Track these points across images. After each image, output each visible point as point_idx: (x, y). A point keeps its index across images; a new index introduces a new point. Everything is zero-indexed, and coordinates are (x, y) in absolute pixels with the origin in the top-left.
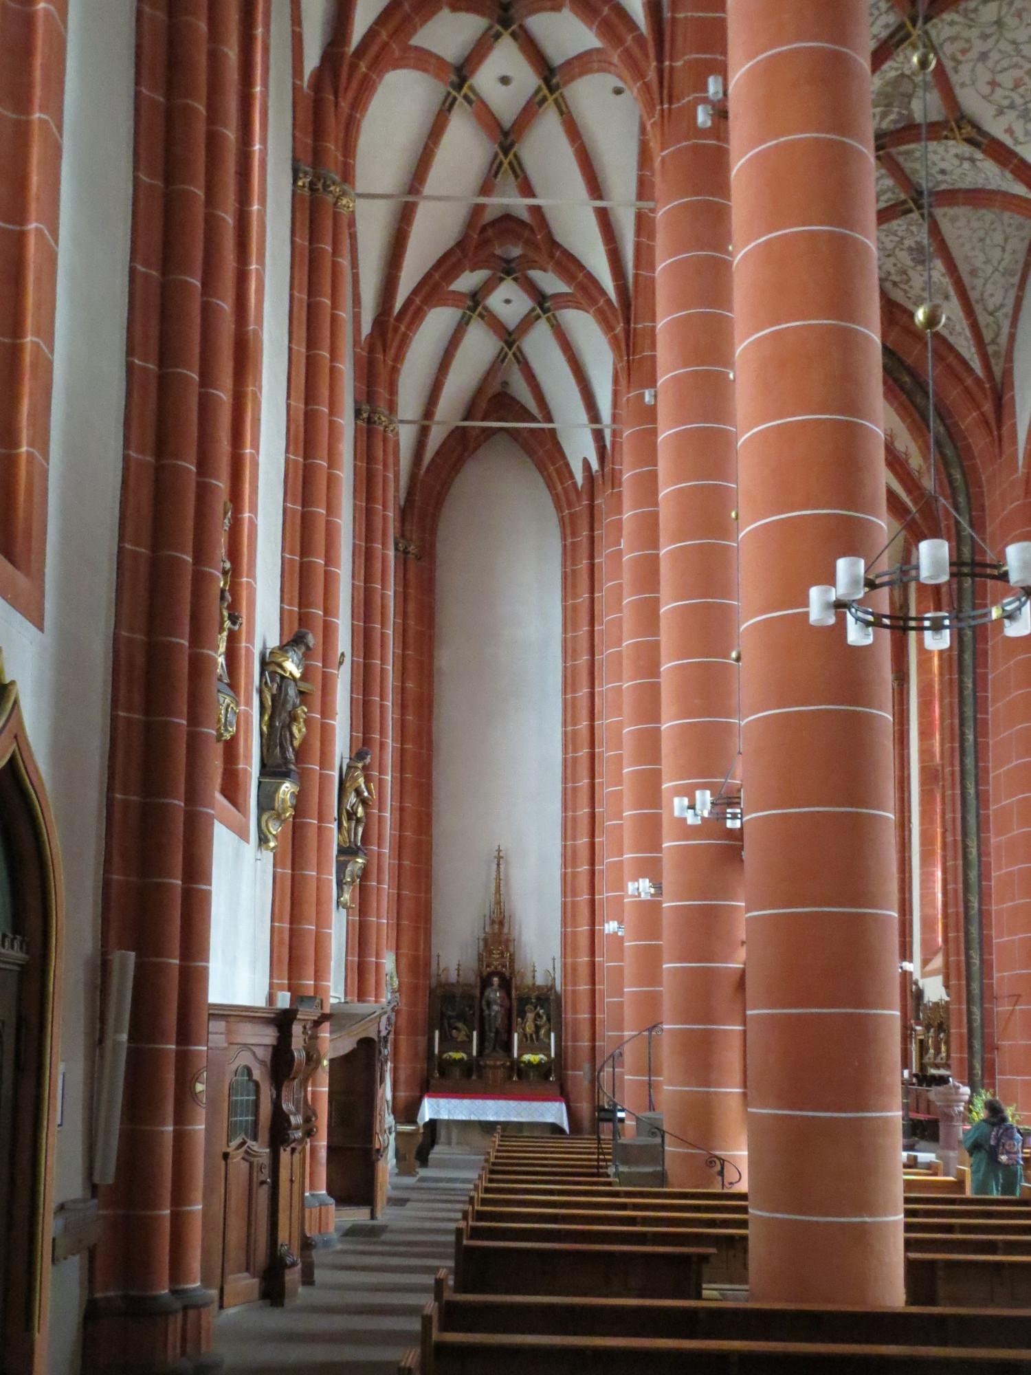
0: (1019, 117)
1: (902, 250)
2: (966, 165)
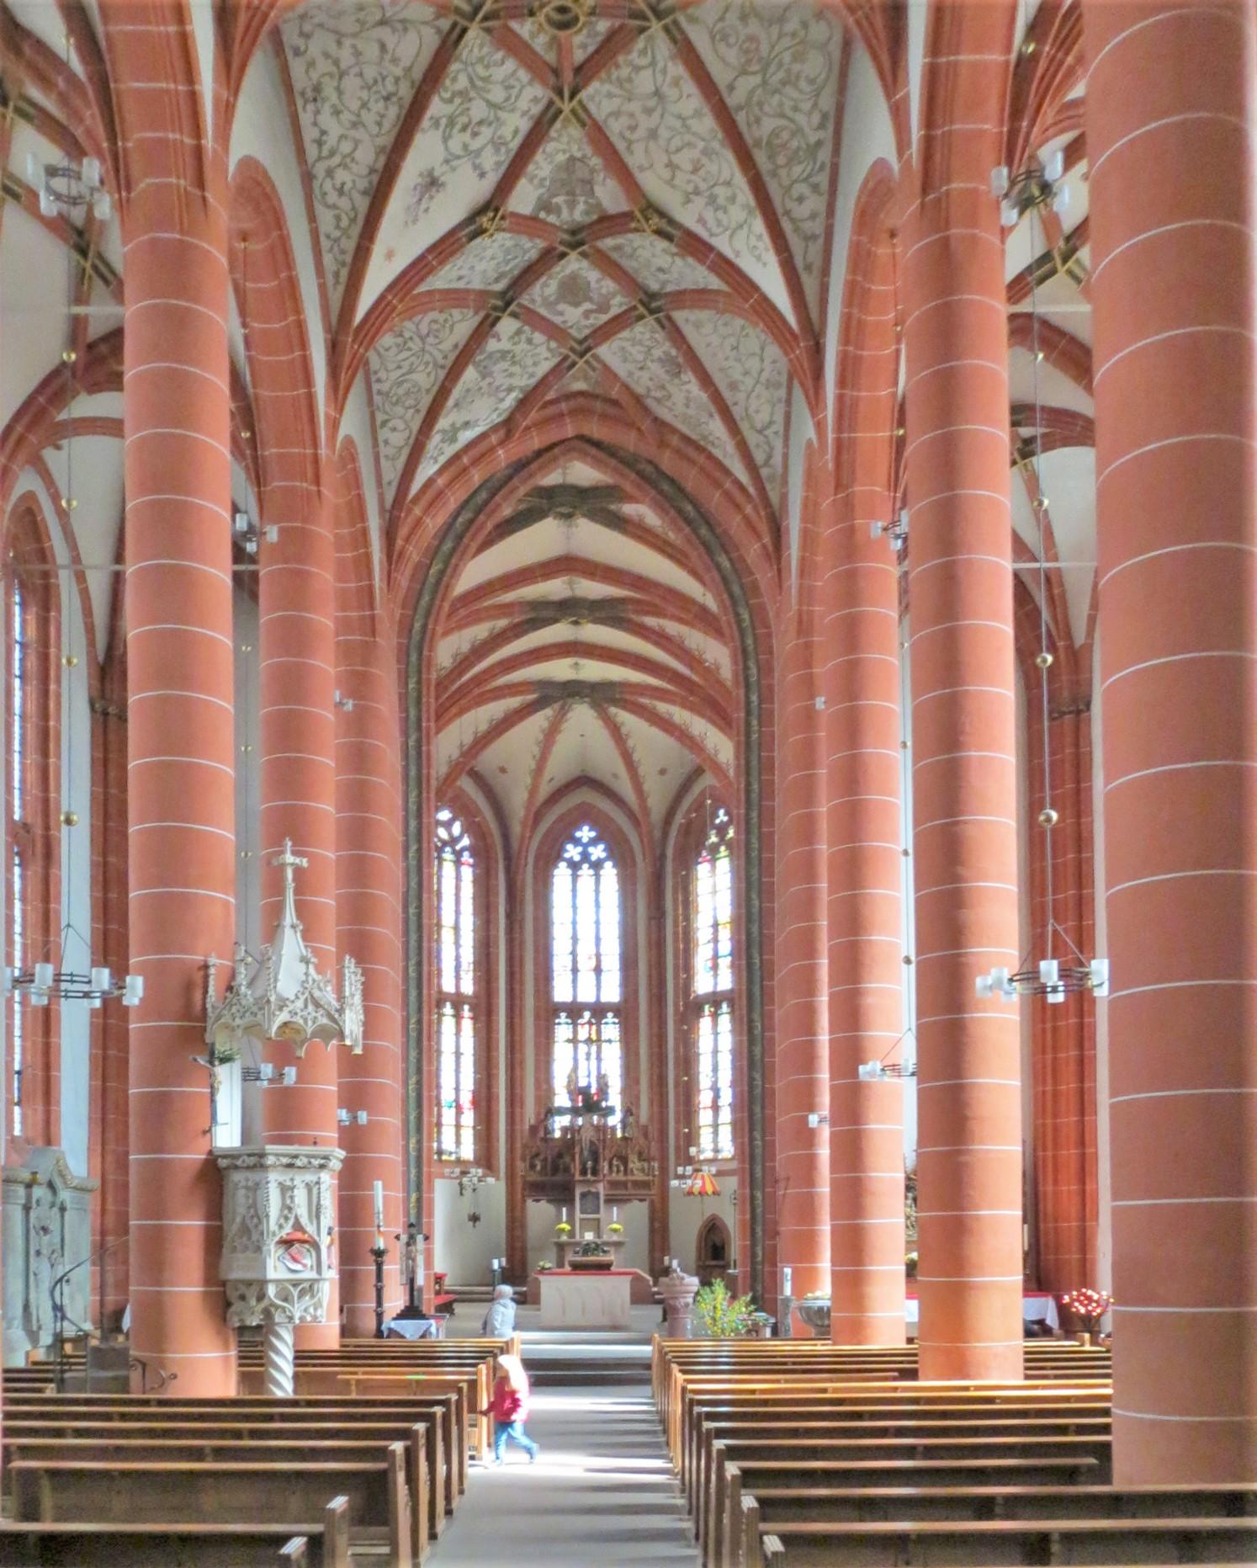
0: (707, 204)
1: (652, 361)
2: (678, 261)
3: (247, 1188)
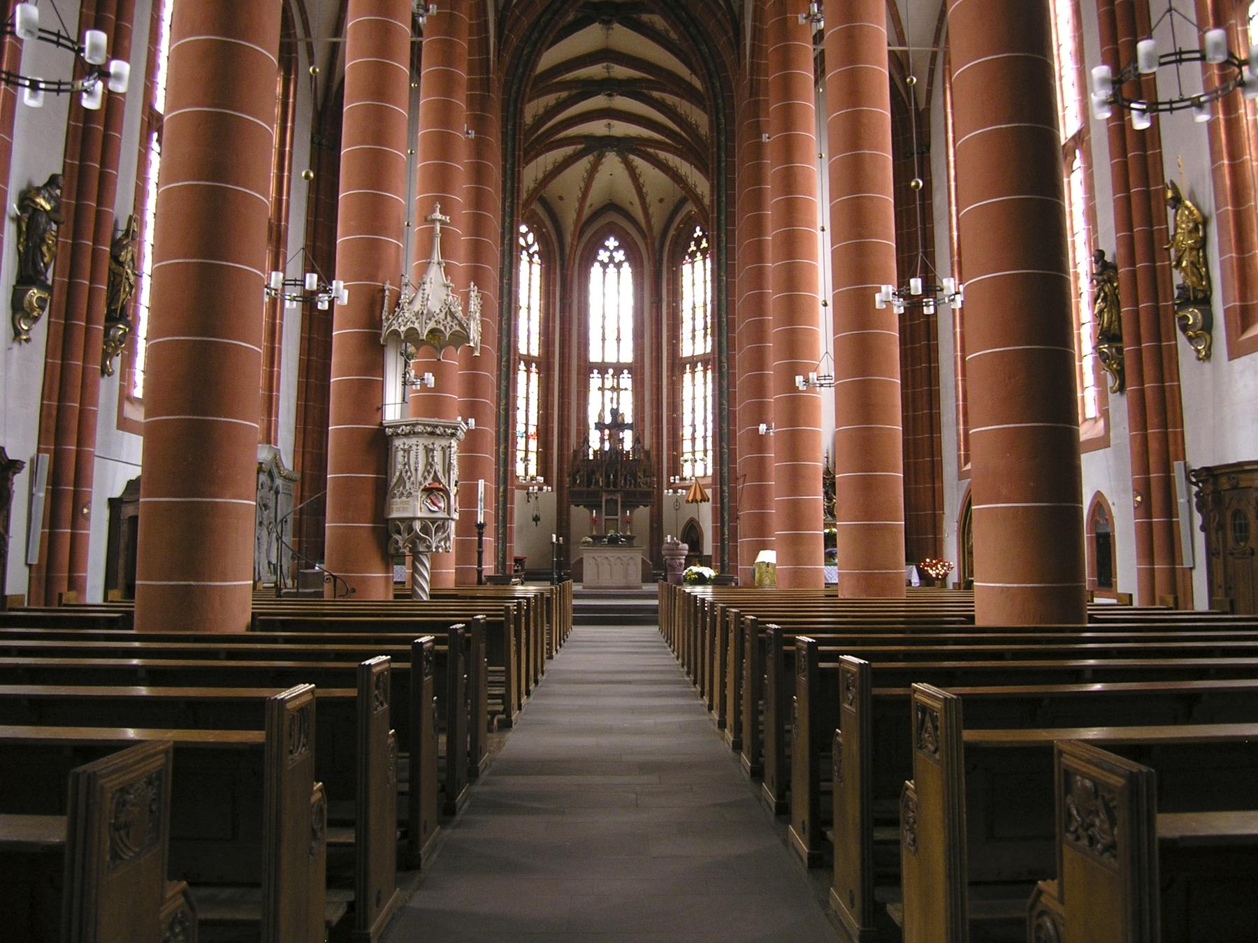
3: (404, 450)
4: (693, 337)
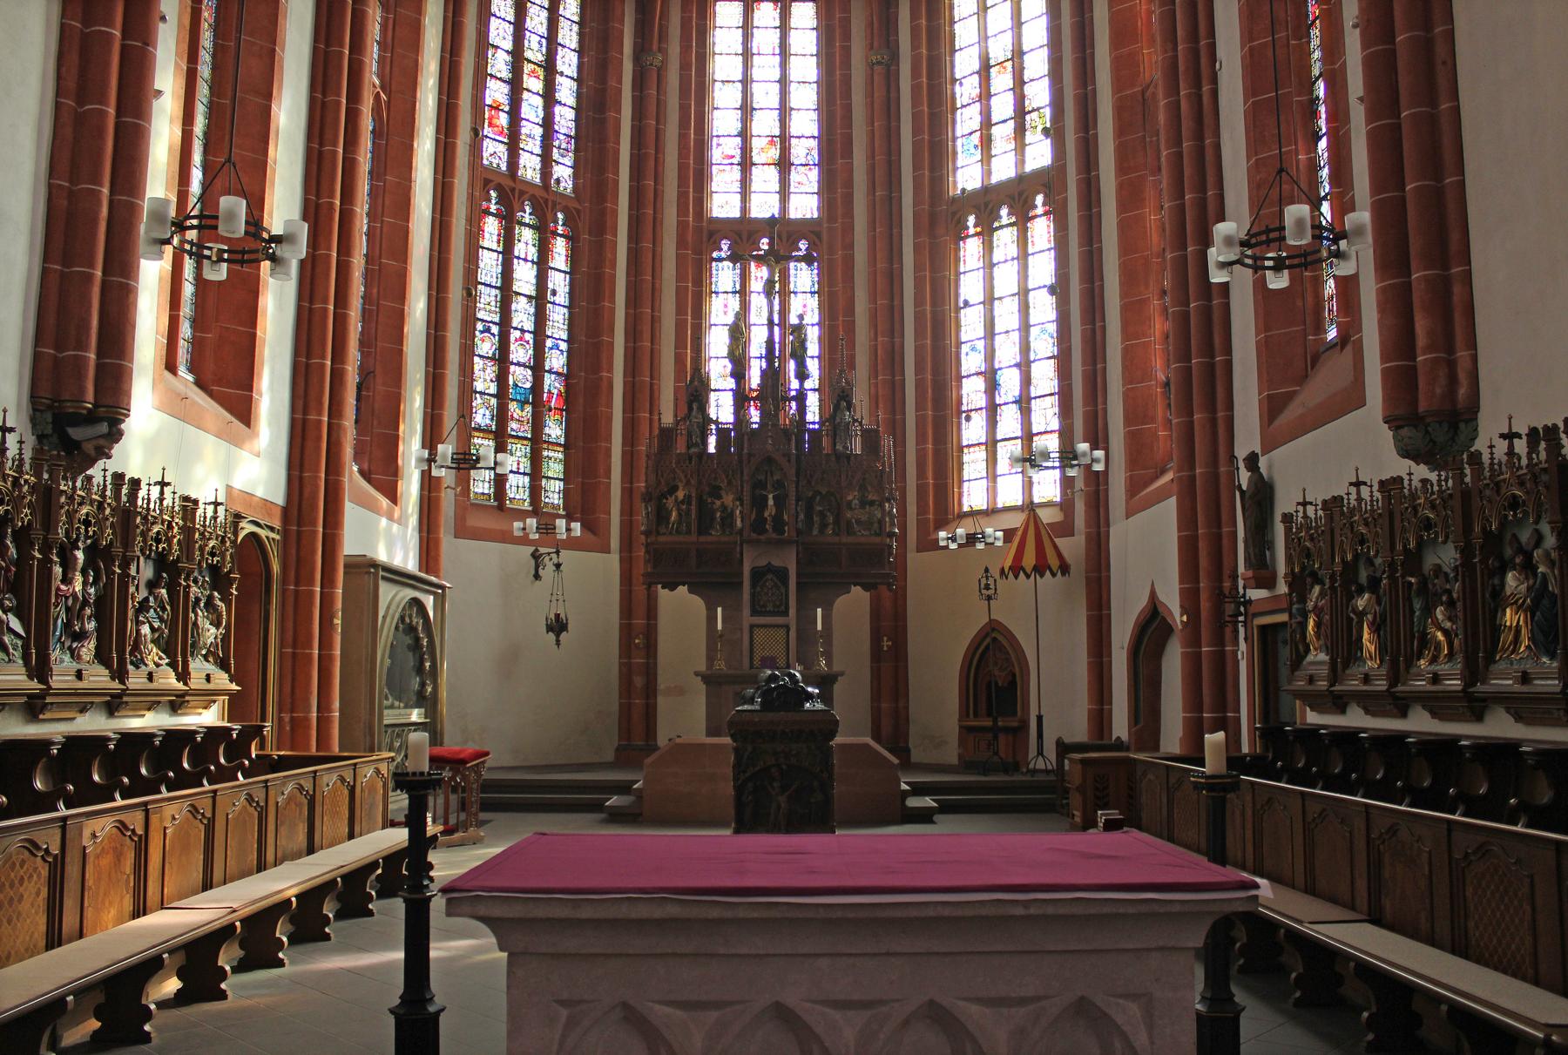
4: (986, 143)
